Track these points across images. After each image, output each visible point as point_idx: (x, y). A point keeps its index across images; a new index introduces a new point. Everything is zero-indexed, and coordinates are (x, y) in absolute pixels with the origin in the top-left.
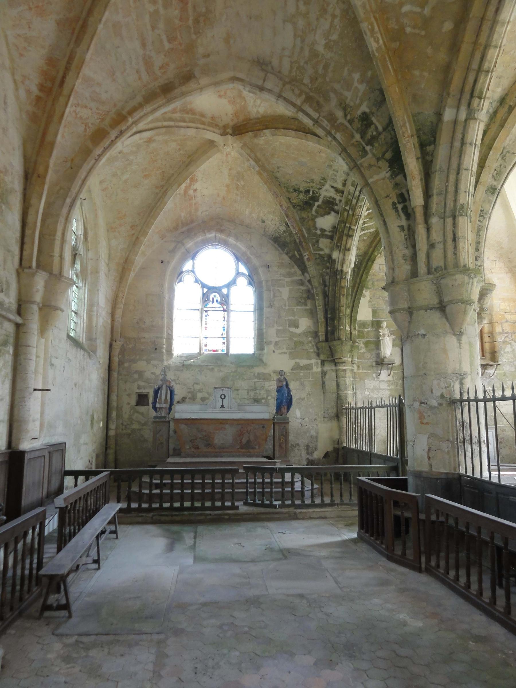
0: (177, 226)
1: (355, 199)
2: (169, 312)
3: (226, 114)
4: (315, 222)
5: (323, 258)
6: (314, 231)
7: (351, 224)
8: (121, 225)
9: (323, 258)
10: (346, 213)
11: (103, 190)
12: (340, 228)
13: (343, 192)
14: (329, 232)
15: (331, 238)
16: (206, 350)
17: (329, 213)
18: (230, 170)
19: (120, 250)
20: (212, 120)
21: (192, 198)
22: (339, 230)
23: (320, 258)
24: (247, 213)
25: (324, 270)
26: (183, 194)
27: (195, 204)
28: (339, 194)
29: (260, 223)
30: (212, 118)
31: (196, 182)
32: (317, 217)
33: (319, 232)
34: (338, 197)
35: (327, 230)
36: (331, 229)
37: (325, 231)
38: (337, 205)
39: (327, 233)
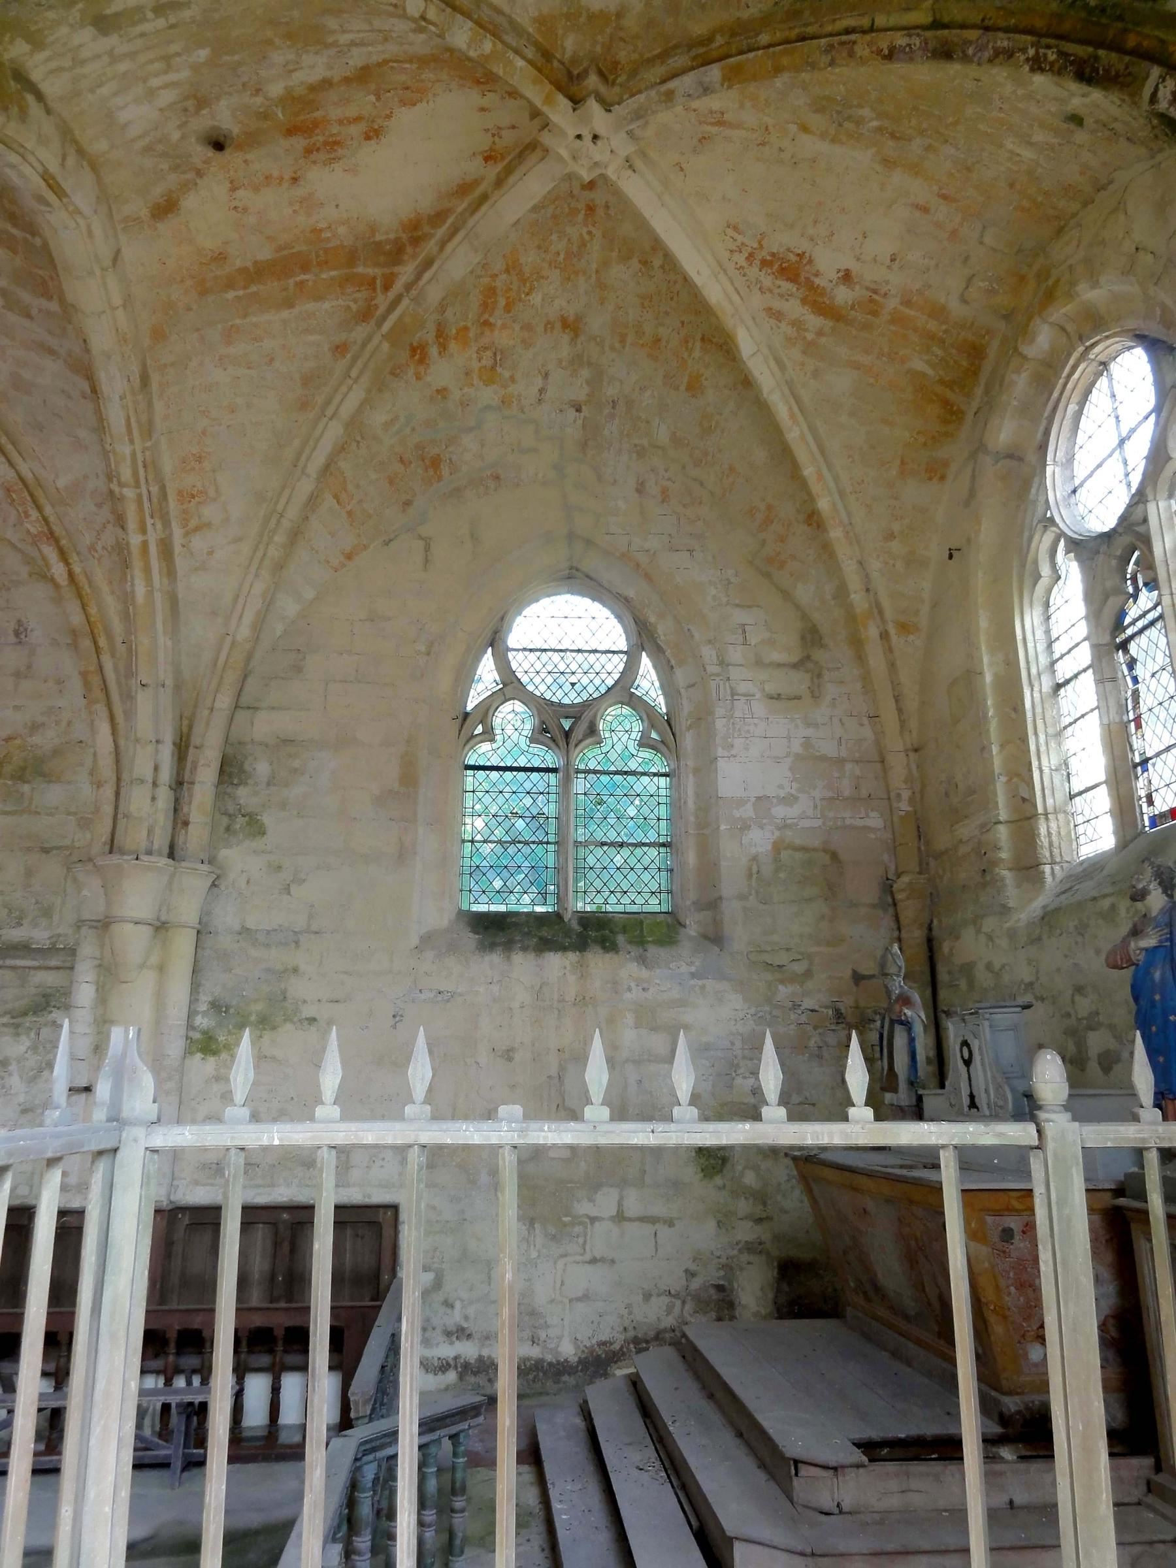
0: (946, 403)
2: (1013, 715)
3: (483, 109)
8: (782, 539)
11: (663, 501)
16: (1154, 820)
18: (805, 129)
19: (834, 598)
20: (503, 158)
21: (871, 300)
24: (1027, 154)
26: (829, 323)
27: (907, 303)
29: (1081, 136)
30: (487, 159)
31: (810, 262)
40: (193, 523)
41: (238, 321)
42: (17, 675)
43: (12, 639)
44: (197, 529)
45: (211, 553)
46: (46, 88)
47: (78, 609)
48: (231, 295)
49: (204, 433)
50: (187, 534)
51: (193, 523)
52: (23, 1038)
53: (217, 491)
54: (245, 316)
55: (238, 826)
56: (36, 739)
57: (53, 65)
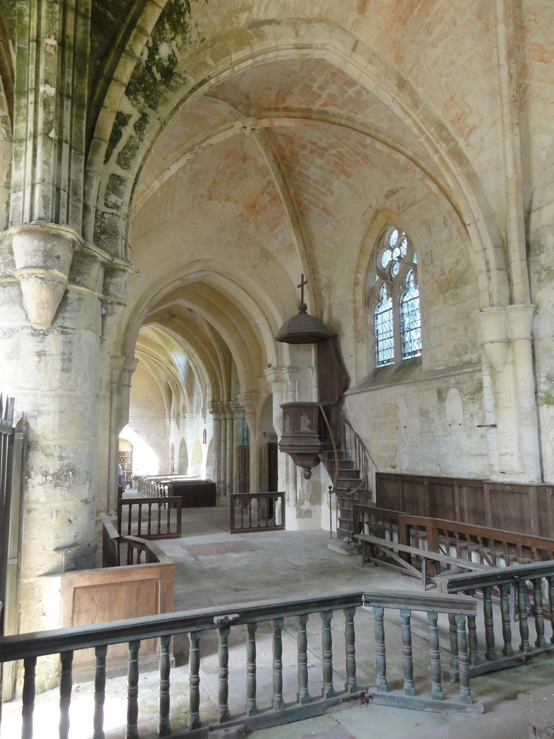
40: (466, 131)
41: (427, 20)
42: (448, 241)
43: (444, 226)
44: (470, 132)
45: (482, 140)
46: (270, 16)
47: (447, 201)
48: (416, 11)
49: (446, 85)
50: (466, 139)
51: (466, 131)
52: (476, 404)
53: (469, 107)
54: (428, 15)
55: (543, 277)
56: (459, 267)
57: (262, 7)
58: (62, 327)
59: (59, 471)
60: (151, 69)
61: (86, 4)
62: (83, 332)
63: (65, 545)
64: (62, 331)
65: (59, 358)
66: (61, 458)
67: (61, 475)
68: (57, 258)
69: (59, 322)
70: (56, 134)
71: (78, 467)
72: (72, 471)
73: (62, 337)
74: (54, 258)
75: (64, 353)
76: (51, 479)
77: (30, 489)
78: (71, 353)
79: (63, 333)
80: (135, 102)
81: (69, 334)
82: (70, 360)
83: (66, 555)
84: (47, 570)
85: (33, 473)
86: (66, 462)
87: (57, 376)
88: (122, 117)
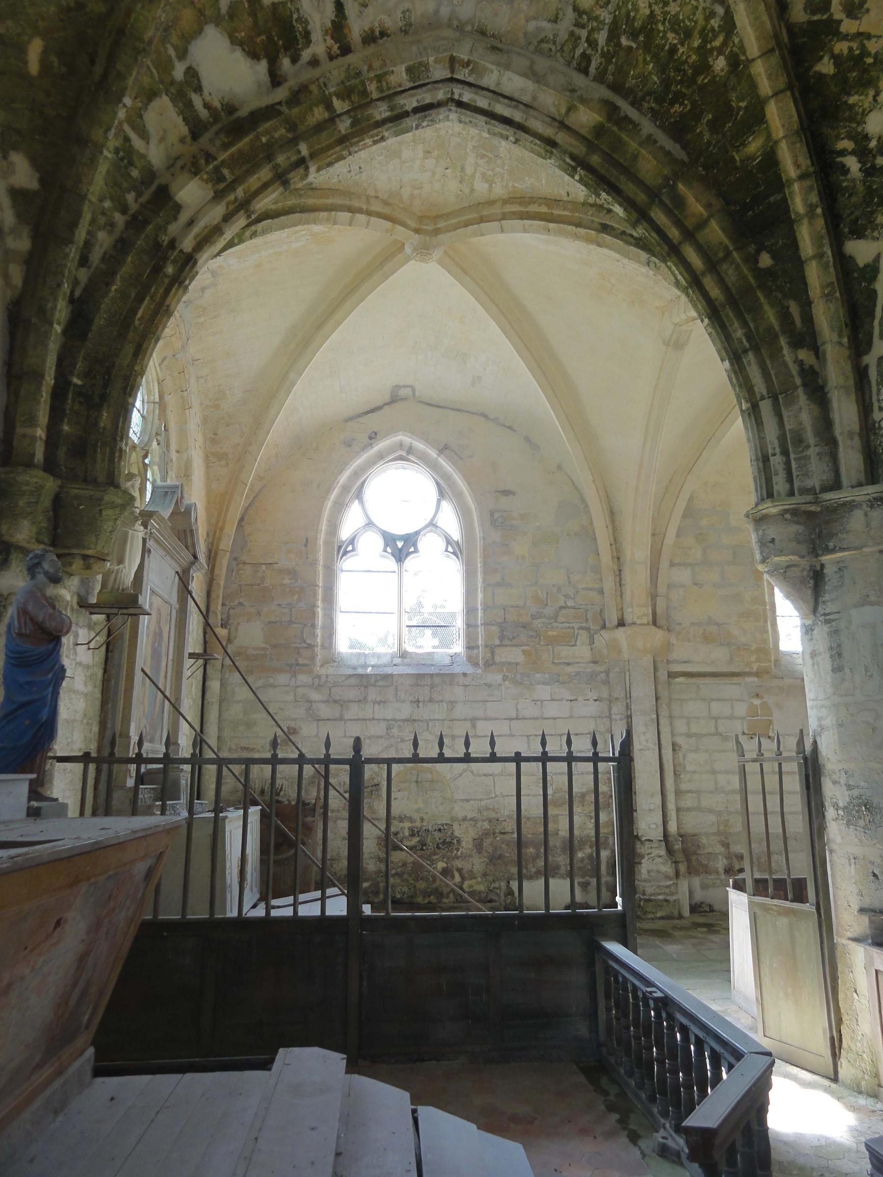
1: (391, 109)
4: (199, 31)
5: (131, 163)
6: (172, 52)
7: (313, 156)
9: (131, 163)
10: (319, 114)
12: (267, 132)
13: (346, 50)
14: (206, 106)
15: (196, 129)
17: (254, 55)
22: (258, 138)
23: (121, 154)
25: (107, 204)
28: (330, 41)
32: (217, 25)
33: (179, 72)
34: (319, 45)
35: (206, 92)
36: (216, 104)
37: (199, 89)
38: (295, 60)
39: (197, 101)
58: (825, 615)
59: (849, 803)
60: (873, 166)
61: (721, 243)
62: (854, 612)
63: (871, 907)
64: (825, 620)
65: (828, 655)
66: (849, 787)
67: (852, 810)
68: (771, 542)
69: (820, 609)
70: (747, 401)
71: (875, 801)
72: (865, 806)
73: (826, 628)
74: (769, 544)
75: (831, 648)
76: (842, 813)
77: (828, 824)
78: (839, 646)
79: (827, 622)
80: (876, 234)
81: (833, 620)
82: (840, 655)
83: (871, 921)
84: (855, 935)
85: (826, 804)
86: (856, 792)
87: (829, 680)
88: (868, 269)
